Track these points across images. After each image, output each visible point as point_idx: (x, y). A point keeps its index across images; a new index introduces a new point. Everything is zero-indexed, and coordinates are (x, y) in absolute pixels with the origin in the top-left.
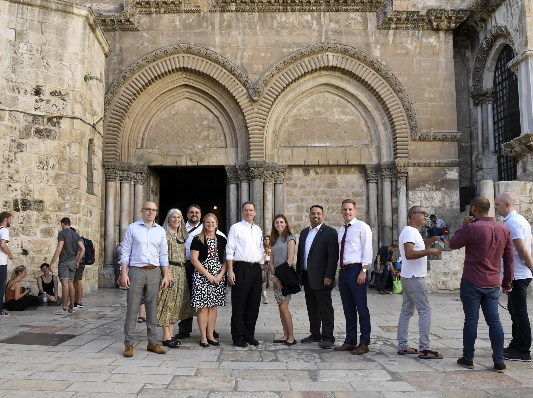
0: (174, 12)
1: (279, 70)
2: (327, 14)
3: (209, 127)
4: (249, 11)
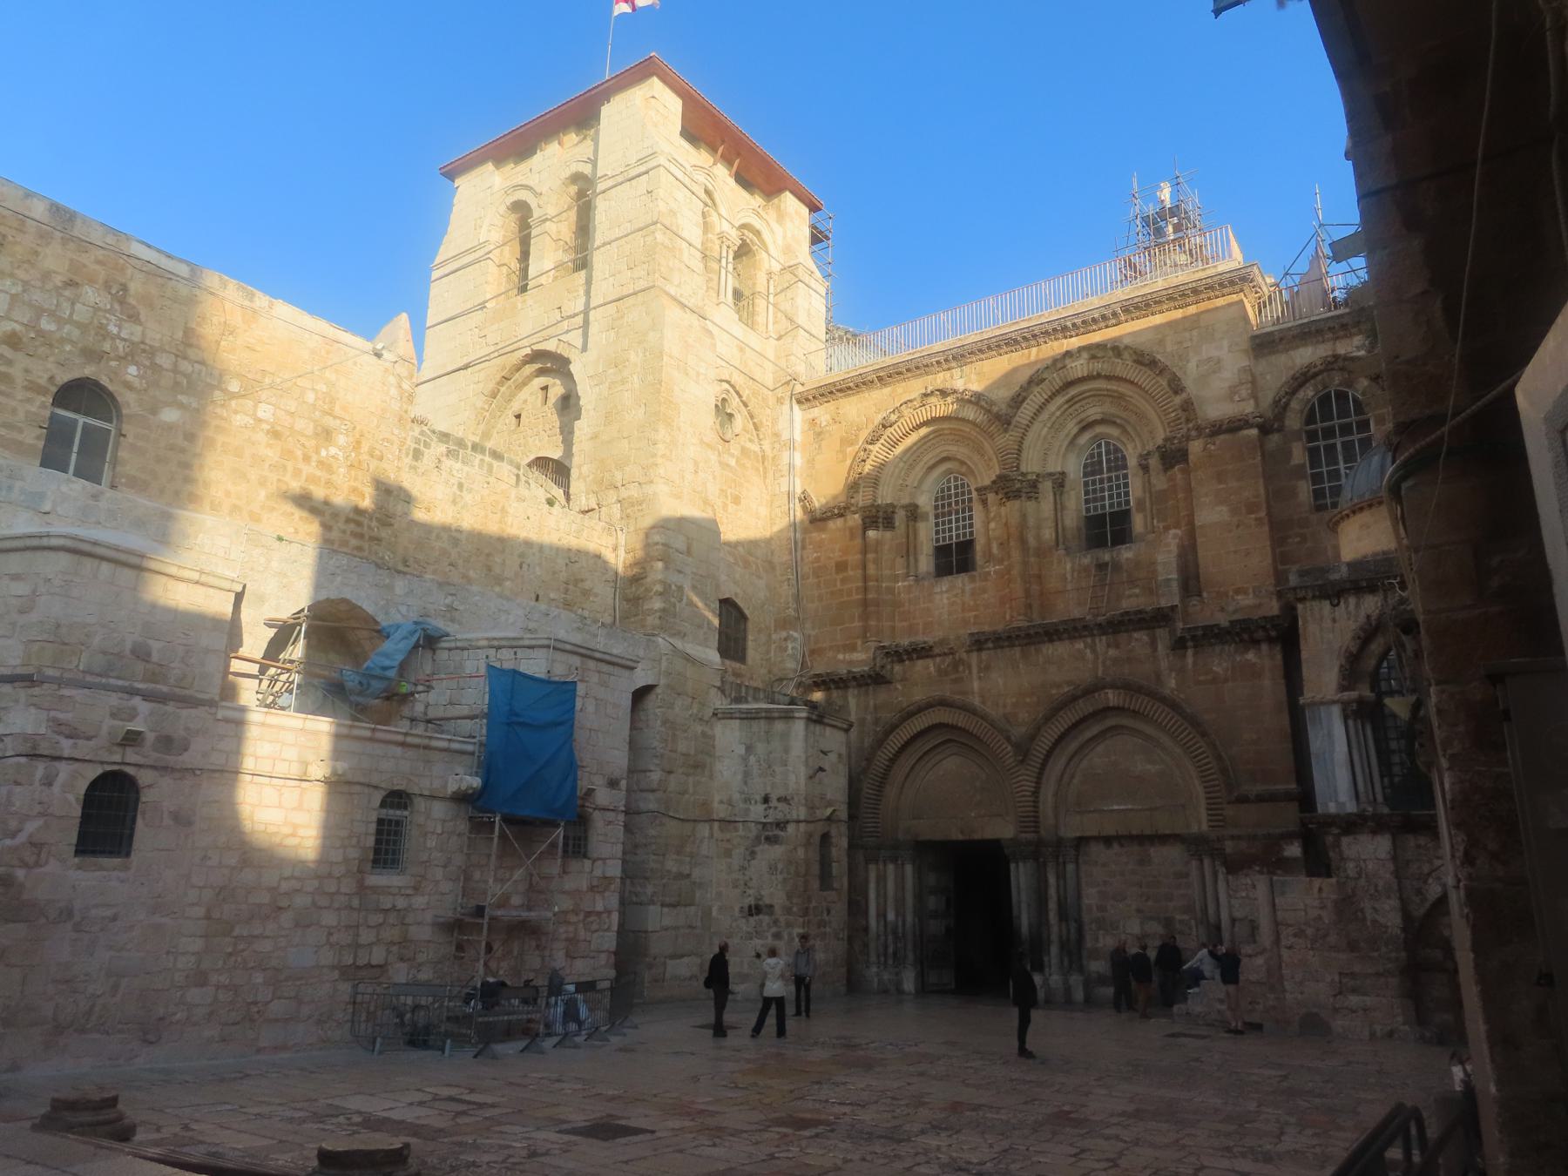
0: (927, 657)
1: (1048, 718)
2: (1104, 638)
4: (1008, 646)
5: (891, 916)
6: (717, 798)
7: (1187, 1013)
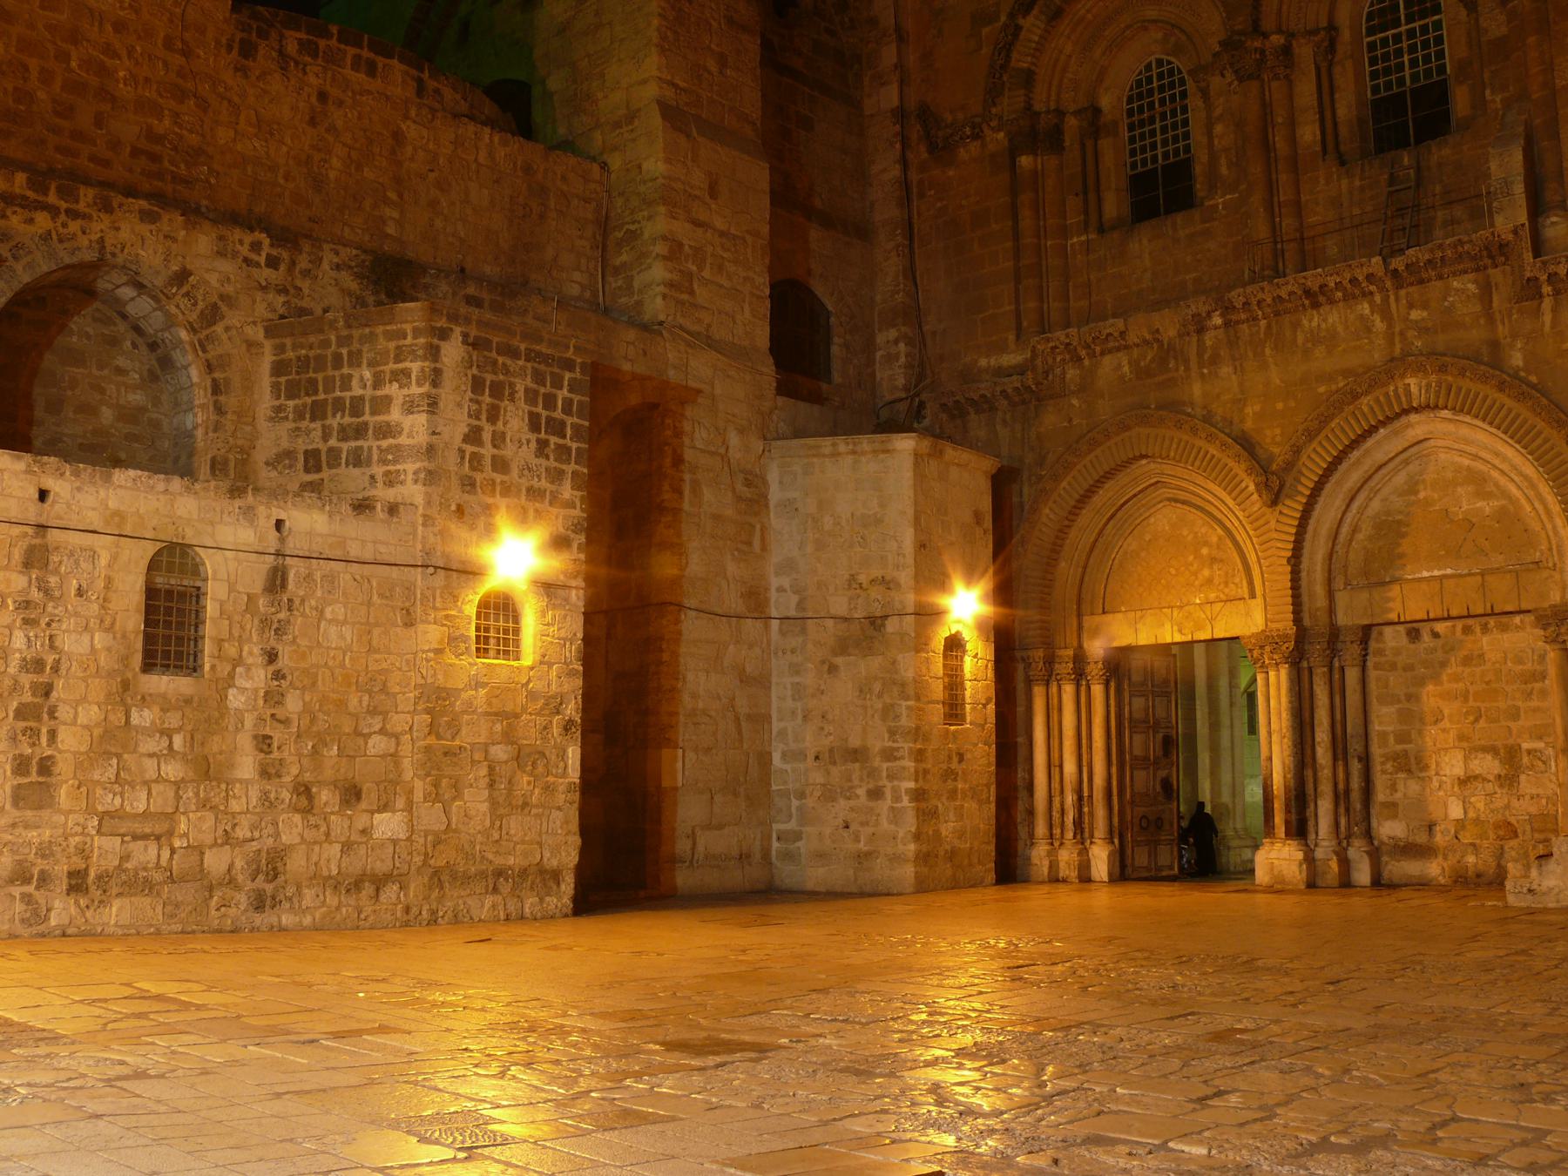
0: (1118, 349)
2: (1402, 293)
3: (1213, 560)
5: (1070, 767)
6: (775, 582)
7: (1530, 891)
